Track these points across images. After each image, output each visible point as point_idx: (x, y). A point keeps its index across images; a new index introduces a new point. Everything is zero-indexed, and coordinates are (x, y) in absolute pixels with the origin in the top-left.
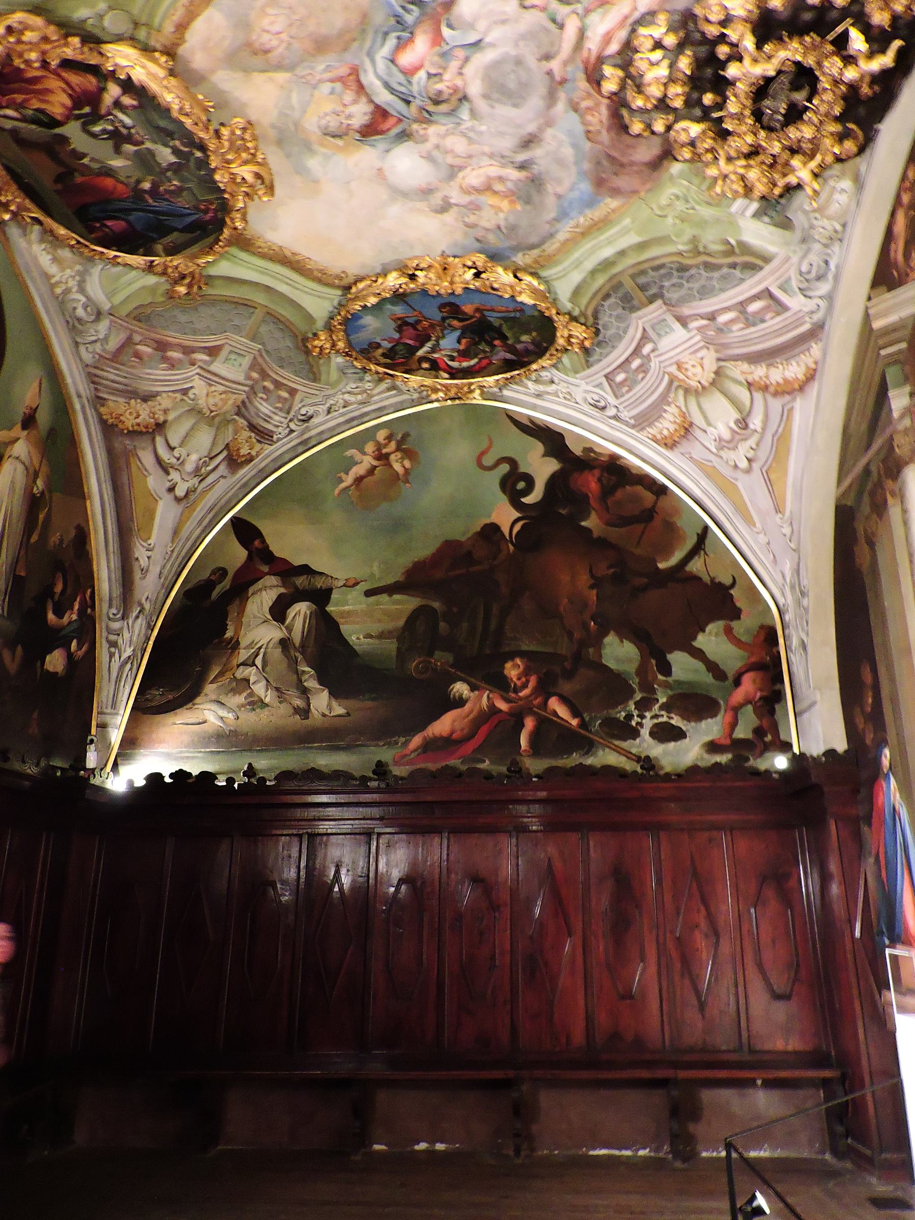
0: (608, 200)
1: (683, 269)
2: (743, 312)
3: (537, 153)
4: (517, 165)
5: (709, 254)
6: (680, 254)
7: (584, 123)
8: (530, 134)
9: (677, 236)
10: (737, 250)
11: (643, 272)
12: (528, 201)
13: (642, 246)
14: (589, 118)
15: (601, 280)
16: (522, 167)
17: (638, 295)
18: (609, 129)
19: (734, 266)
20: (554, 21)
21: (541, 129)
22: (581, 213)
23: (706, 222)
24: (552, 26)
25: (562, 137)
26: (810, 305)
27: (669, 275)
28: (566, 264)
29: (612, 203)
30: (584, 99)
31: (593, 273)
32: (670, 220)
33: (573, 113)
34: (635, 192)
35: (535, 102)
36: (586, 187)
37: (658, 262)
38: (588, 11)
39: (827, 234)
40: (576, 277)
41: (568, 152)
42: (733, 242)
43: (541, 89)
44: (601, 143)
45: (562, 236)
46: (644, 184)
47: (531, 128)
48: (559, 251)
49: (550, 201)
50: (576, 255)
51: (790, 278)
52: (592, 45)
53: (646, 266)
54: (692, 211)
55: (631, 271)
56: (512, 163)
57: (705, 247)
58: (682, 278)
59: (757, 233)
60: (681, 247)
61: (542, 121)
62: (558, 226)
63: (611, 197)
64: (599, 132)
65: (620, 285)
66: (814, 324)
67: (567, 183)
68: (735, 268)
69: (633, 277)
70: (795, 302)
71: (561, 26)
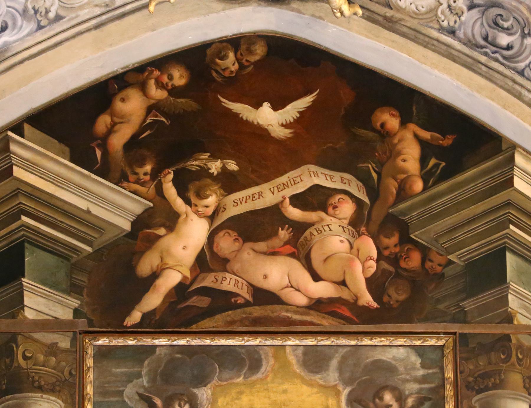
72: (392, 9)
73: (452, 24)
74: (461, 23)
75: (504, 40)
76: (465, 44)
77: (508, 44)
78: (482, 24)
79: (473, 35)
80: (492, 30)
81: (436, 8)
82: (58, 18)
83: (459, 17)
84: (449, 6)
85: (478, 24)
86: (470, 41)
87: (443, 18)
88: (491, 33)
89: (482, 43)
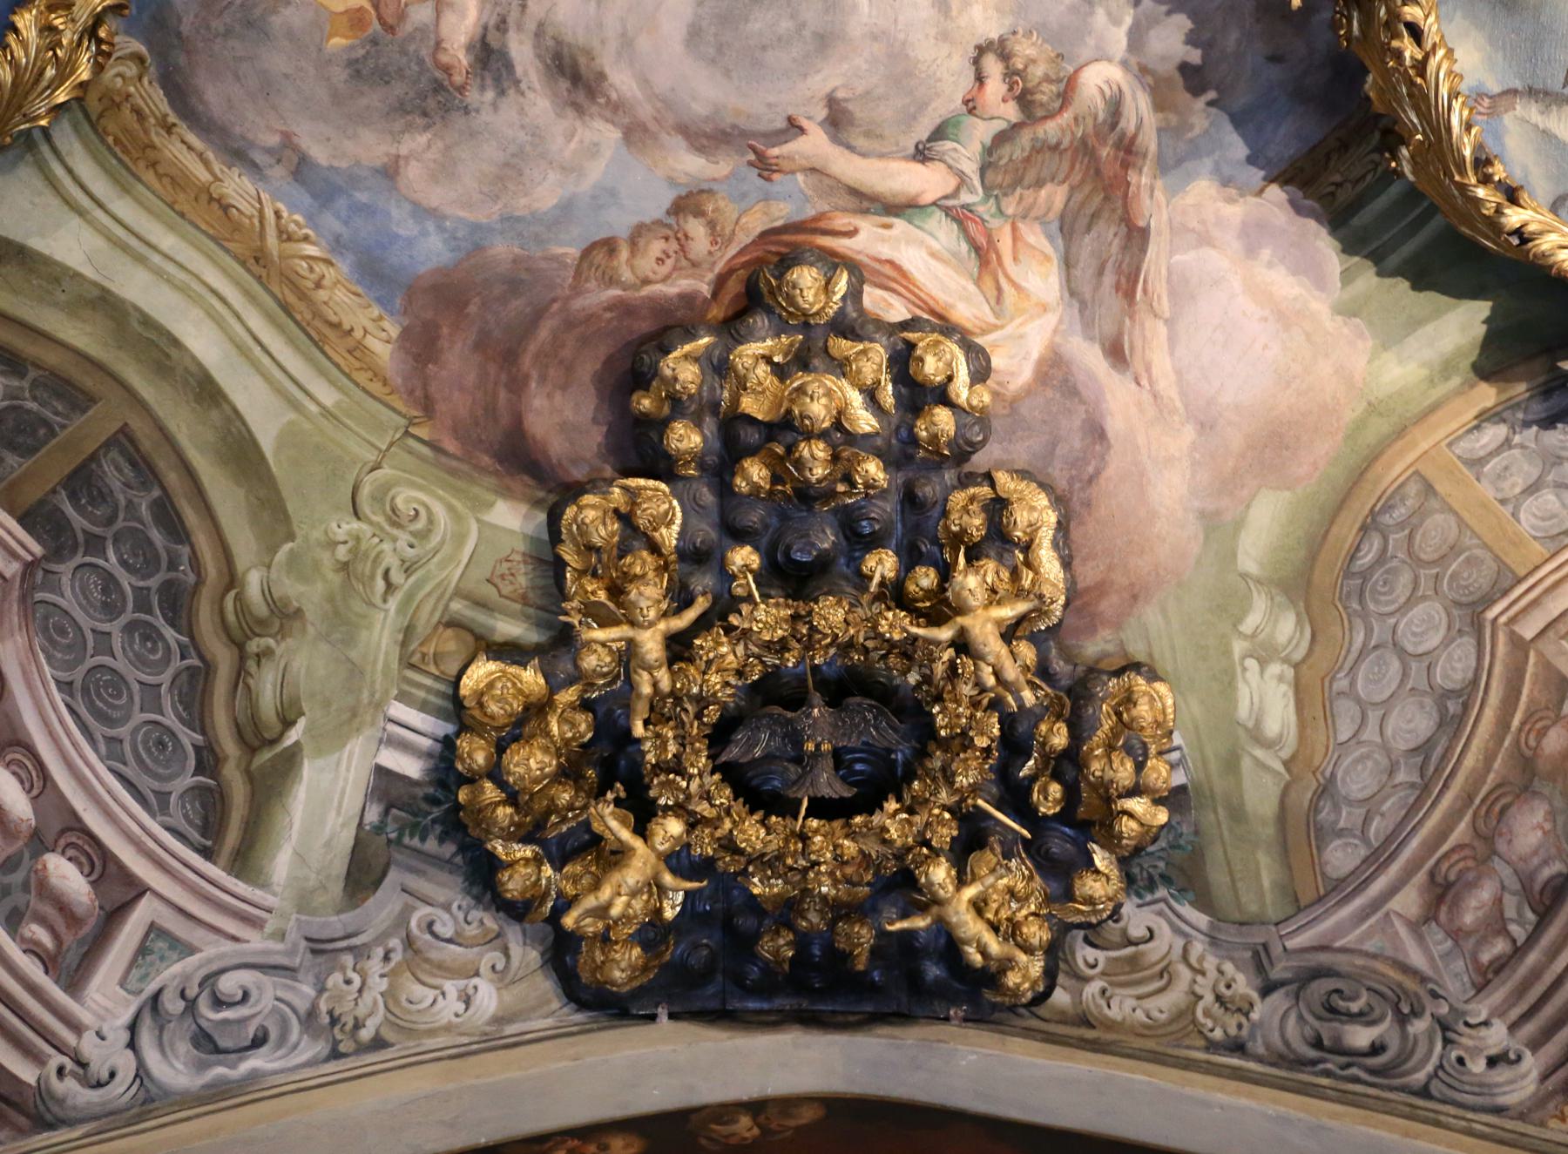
0: (394, 331)
1: (177, 603)
2: (39, 842)
3: (539, 101)
4: (493, 39)
5: (240, 673)
6: (232, 580)
7: (638, 234)
8: (602, 76)
9: (293, 557)
10: (266, 756)
11: (145, 471)
12: (366, 70)
13: (242, 453)
14: (657, 247)
15: (79, 334)
16: (489, 56)
17: (51, 466)
18: (624, 309)
19: (208, 760)
20: (939, 133)
21: (616, 108)
22: (337, 244)
23: (349, 641)
24: (923, 131)
25: (596, 171)
26: (106, 1053)
27: (143, 560)
28: (124, 208)
29: (382, 340)
30: (712, 225)
31: (103, 304)
32: (346, 527)
33: (667, 198)
34: (428, 407)
35: (708, 92)
36: (431, 251)
37: (191, 517)
38: (961, 217)
39: (344, 1008)
40: (70, 245)
41: (545, 193)
42: (293, 735)
43: (759, 104)
44: (577, 290)
45: (237, 187)
46: (456, 431)
47: (621, 81)
48: (178, 180)
49: (371, 147)
50: (167, 241)
51: (191, 950)
52: (869, 239)
53: (172, 478)
54: (380, 584)
55: (139, 426)
56: (502, 25)
57: (264, 655)
58: (143, 604)
59: (325, 802)
60: (253, 582)
61: (645, 112)
62: (278, 173)
63: (406, 333)
64: (612, 281)
65: (77, 399)
66: (41, 1090)
67: (435, 196)
68: (199, 770)
69: (123, 440)
70: (106, 1000)
71: (922, 154)
72: (1093, 1027)
73: (1233, 1031)
74: (1254, 1026)
75: (1360, 1037)
76: (1273, 1065)
77: (1373, 1044)
78: (1301, 1017)
79: (1287, 1043)
80: (1326, 1025)
81: (1191, 1009)
82: (378, 1043)
83: (1247, 1015)
84: (1219, 998)
85: (1292, 1021)
86: (1281, 1056)
87: (1210, 1024)
88: (1326, 1030)
89: (1313, 1054)
